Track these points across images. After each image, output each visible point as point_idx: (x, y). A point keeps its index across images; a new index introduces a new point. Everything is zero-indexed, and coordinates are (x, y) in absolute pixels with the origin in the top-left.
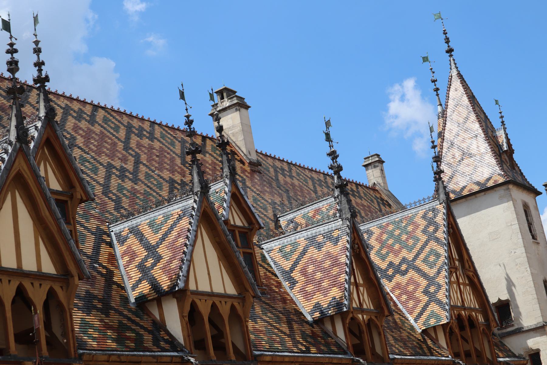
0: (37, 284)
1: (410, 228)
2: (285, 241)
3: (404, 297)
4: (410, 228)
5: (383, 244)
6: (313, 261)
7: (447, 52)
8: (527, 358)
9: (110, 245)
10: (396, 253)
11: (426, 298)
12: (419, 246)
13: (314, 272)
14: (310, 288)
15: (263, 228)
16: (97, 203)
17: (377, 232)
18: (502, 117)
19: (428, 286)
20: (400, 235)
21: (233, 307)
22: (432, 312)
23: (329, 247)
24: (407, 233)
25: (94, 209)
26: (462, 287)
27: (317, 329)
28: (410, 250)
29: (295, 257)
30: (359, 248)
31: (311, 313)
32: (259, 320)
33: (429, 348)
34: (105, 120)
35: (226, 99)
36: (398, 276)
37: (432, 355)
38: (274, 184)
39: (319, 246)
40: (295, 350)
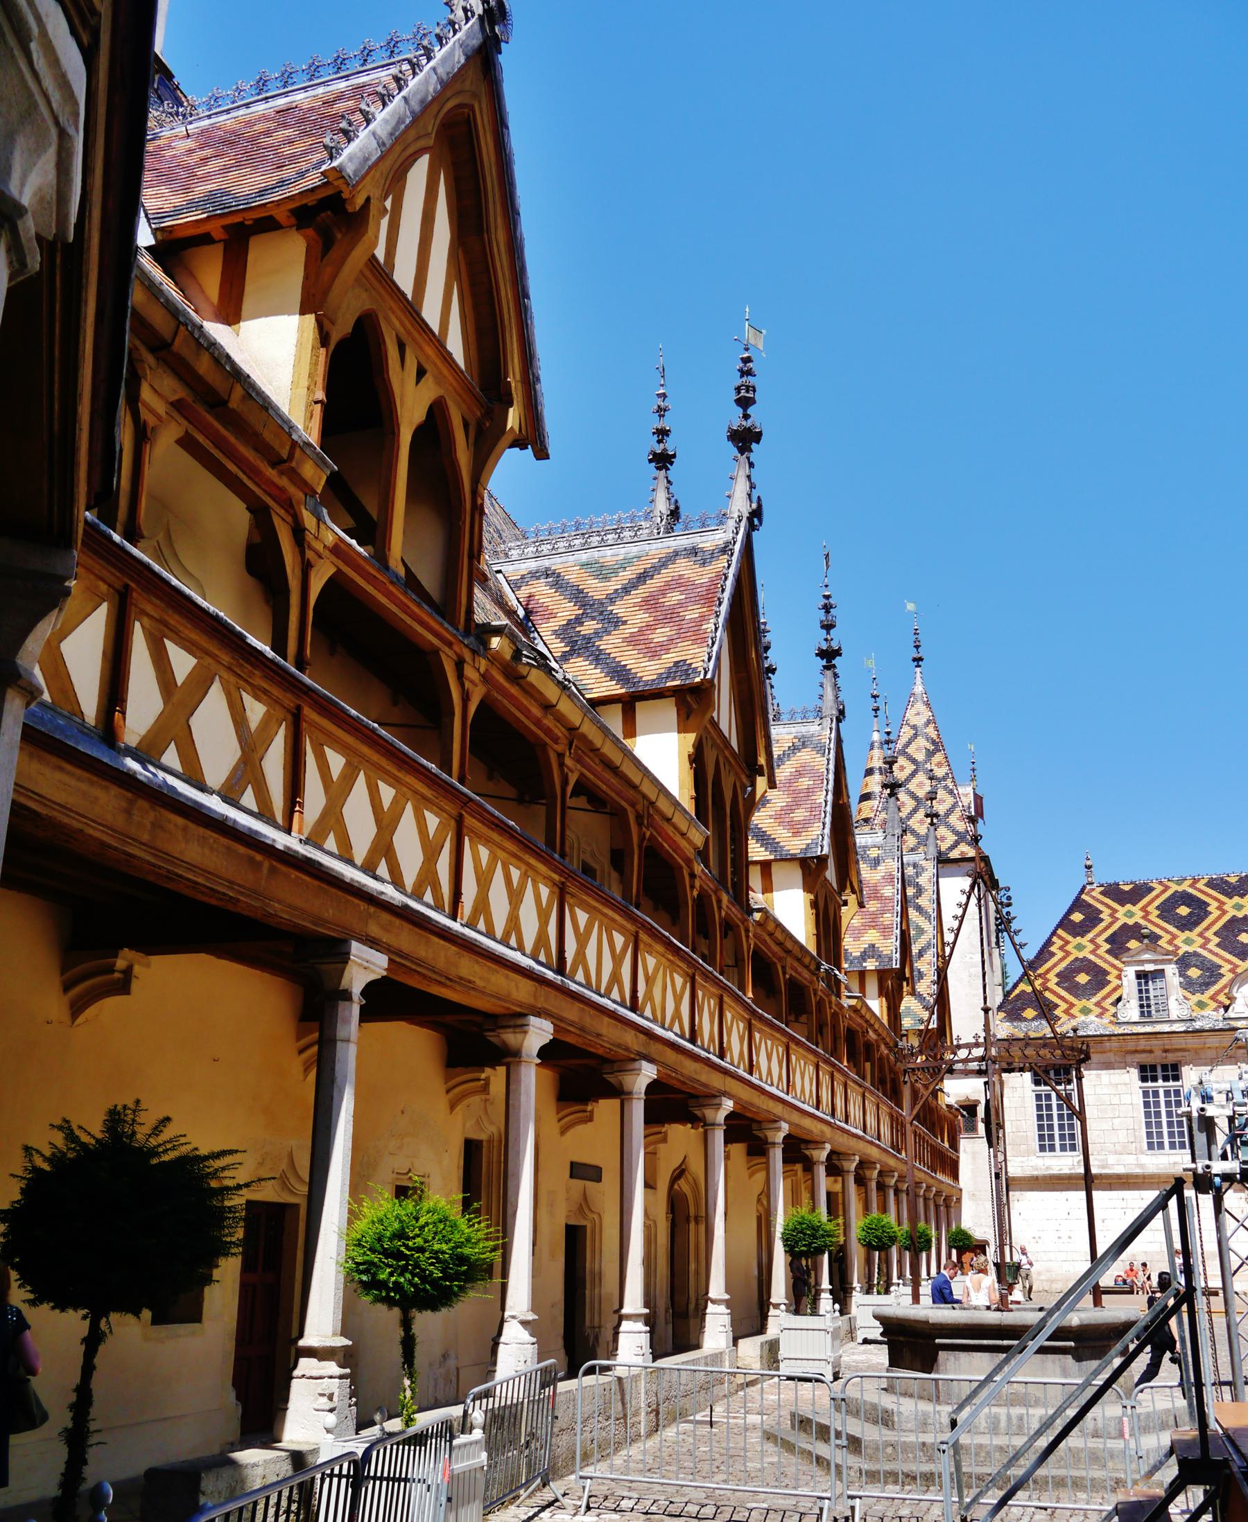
7: (914, 660)
18: (974, 770)
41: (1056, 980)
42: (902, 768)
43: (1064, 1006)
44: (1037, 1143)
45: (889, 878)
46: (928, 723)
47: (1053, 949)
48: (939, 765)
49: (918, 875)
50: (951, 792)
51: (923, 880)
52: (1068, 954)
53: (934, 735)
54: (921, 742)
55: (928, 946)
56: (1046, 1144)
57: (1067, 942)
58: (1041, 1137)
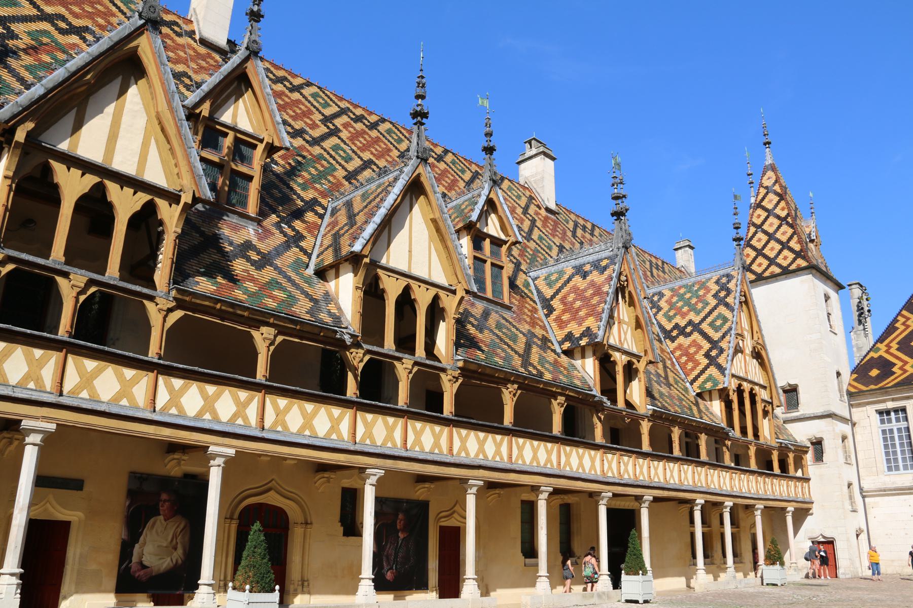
0: (129, 191)
1: (701, 293)
2: (553, 269)
3: (684, 359)
4: (701, 293)
5: (672, 305)
6: (575, 289)
7: (765, 144)
8: (809, 445)
9: (322, 217)
10: (684, 315)
11: (706, 361)
12: (707, 310)
13: (575, 300)
14: (565, 317)
15: (520, 243)
16: (329, 181)
17: (668, 293)
19: (710, 350)
20: (690, 298)
21: (436, 298)
23: (595, 277)
24: (697, 297)
26: (747, 358)
27: (564, 359)
28: (698, 313)
29: (559, 285)
30: (627, 280)
31: (561, 343)
32: (486, 331)
33: (700, 411)
34: (389, 131)
35: (533, 149)
38: (569, 234)
39: (585, 275)
40: (522, 370)
41: (897, 346)
42: (759, 216)
43: (900, 364)
46: (776, 182)
47: (897, 325)
48: (783, 209)
49: (728, 282)
50: (791, 226)
51: (731, 286)
52: (908, 327)
53: (779, 191)
54: (771, 196)
55: (730, 329)
57: (908, 319)
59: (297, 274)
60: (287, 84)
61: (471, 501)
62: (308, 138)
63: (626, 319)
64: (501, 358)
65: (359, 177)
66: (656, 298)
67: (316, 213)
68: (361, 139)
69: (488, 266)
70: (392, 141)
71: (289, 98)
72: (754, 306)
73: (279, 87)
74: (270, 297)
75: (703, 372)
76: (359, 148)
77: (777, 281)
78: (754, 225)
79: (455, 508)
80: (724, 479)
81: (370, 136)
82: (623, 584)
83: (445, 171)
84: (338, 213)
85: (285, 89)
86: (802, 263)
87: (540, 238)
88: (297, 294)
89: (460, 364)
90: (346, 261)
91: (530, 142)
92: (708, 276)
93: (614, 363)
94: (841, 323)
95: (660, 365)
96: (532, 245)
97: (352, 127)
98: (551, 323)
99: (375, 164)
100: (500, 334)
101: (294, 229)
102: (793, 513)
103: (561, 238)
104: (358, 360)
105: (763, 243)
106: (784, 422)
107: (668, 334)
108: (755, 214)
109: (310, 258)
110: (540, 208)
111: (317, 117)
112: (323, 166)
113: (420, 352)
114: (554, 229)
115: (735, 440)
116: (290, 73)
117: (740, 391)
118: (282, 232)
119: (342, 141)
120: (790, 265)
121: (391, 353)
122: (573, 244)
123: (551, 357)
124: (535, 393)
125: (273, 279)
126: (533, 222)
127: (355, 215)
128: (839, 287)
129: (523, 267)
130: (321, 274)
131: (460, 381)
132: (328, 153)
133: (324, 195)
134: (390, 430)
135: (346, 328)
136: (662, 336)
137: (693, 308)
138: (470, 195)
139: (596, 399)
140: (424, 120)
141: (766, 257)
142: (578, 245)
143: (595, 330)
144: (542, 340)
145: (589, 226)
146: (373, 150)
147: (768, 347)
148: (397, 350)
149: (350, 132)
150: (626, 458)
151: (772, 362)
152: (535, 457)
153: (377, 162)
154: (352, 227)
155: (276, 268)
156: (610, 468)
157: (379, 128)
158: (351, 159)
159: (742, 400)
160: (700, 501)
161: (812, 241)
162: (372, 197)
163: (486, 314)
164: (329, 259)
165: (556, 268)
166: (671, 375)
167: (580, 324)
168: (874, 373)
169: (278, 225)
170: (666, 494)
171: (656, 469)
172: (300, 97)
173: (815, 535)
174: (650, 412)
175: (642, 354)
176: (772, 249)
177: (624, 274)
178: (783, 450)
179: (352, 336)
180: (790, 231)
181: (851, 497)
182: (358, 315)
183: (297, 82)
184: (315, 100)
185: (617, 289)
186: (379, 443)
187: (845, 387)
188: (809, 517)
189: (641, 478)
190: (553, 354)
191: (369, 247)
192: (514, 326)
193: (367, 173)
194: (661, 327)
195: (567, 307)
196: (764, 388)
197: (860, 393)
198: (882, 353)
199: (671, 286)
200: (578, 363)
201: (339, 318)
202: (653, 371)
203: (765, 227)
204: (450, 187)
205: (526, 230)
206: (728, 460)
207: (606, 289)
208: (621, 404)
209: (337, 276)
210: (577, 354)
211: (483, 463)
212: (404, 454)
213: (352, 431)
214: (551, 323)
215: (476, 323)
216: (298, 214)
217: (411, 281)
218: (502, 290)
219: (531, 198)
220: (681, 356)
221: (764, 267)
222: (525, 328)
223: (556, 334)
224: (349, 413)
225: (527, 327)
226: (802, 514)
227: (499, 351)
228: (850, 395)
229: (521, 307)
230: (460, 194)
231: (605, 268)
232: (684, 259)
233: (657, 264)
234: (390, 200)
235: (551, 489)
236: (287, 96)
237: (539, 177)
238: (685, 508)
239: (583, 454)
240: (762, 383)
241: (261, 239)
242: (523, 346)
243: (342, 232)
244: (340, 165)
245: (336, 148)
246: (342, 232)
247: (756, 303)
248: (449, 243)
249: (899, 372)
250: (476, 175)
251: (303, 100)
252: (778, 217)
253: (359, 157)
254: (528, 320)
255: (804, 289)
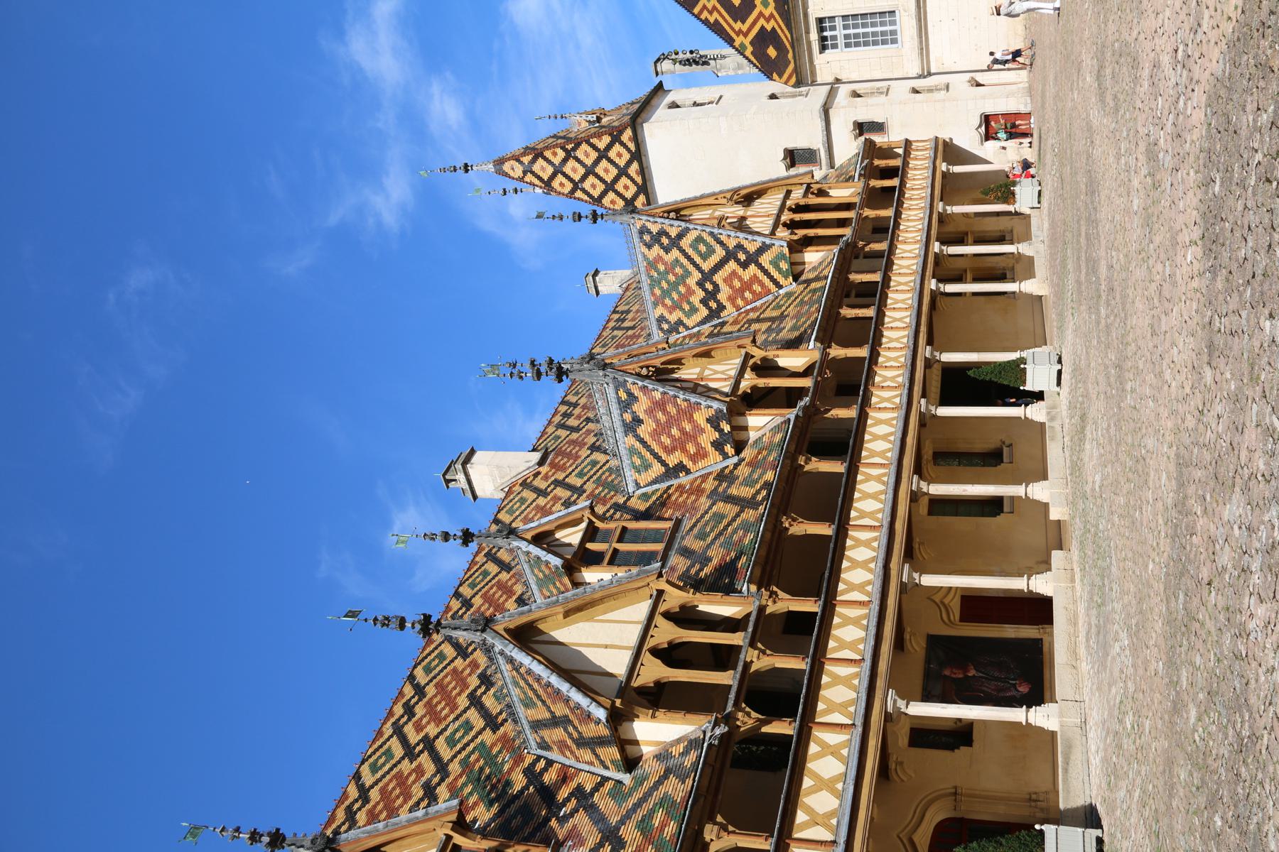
1: (662, 268)
2: (626, 462)
3: (748, 295)
4: (662, 268)
5: (676, 306)
6: (656, 434)
7: (467, 171)
8: (862, 139)
9: (550, 763)
10: (690, 292)
11: (753, 268)
13: (670, 435)
14: (691, 449)
16: (500, 752)
17: (660, 311)
19: (737, 261)
20: (668, 282)
21: (668, 615)
22: (771, 262)
23: (640, 408)
25: (503, 763)
26: (749, 213)
27: (747, 453)
29: (648, 455)
30: (647, 367)
31: (726, 456)
32: (709, 553)
33: (817, 279)
34: (428, 670)
36: (719, 296)
37: (826, 278)
38: (575, 436)
39: (638, 421)
40: (761, 508)
42: (562, 185)
43: (762, 22)
44: (890, 46)
45: (644, 388)
46: (518, 160)
47: (712, 20)
48: (555, 154)
49: (649, 232)
50: (578, 145)
51: (654, 229)
53: (530, 157)
55: (711, 234)
56: (890, 39)
57: (705, 7)
58: (884, 42)
59: (630, 795)
60: (356, 806)
61: (929, 580)
62: (436, 779)
63: (697, 370)
64: (745, 536)
65: (494, 713)
66: (665, 326)
67: (545, 770)
68: (439, 708)
69: (622, 547)
70: (441, 666)
71: (378, 803)
72: (682, 201)
73: (361, 817)
74: (662, 830)
75: (766, 272)
76: (452, 712)
77: (649, 167)
78: (573, 191)
79: (937, 600)
80: (906, 251)
81: (435, 696)
82: (1037, 389)
83: (485, 597)
84: (547, 739)
85: (364, 810)
86: (627, 135)
87: (581, 475)
88: (657, 795)
89: (753, 588)
90: (616, 730)
91: (448, 482)
92: (640, 257)
93: (754, 388)
94: (706, 88)
95: (755, 326)
96: (589, 487)
97: (421, 719)
98: (699, 468)
99: (475, 690)
100: (712, 535)
101: (568, 799)
102: (949, 164)
103: (581, 448)
104: (746, 719)
105: (597, 182)
106: (832, 167)
107: (714, 314)
108: (559, 189)
109: (608, 779)
110: (537, 475)
111: (406, 766)
112: (478, 760)
113: (737, 639)
114: (569, 455)
115: (856, 233)
116: (341, 802)
117: (792, 225)
118: (572, 815)
119: (441, 733)
120: (628, 150)
121: (738, 676)
122: (589, 432)
123: (743, 471)
124: (793, 492)
125: (638, 826)
126: (557, 483)
127: (554, 717)
128: (659, 89)
129: (621, 501)
130: (630, 763)
131: (775, 589)
132: (459, 752)
133: (519, 759)
134: (837, 680)
135: (704, 732)
136: (716, 321)
137: (682, 279)
138: (526, 566)
139: (800, 414)
140: (434, 620)
141: (616, 179)
142: (591, 426)
143: (711, 412)
144: (721, 482)
145: (563, 409)
146: (454, 693)
147: (736, 185)
148: (734, 668)
149: (428, 723)
150: (877, 379)
151: (755, 181)
152: (874, 496)
153: (471, 688)
154: (570, 722)
155: (622, 822)
156: (888, 400)
157: (423, 684)
158: (467, 722)
159: (804, 223)
160: (933, 284)
161: (599, 119)
162: (531, 694)
163: (686, 552)
164: (612, 753)
165: (624, 458)
166: (768, 314)
167: (703, 431)
168: (772, 52)
169: (563, 820)
170: (923, 329)
171: (891, 340)
172: (377, 788)
173: (977, 137)
174: (819, 345)
175: (743, 351)
176: (606, 171)
177: (638, 370)
178: (871, 172)
179: (716, 724)
180: (584, 147)
181: (930, 91)
182: (689, 716)
183: (353, 792)
184: (381, 768)
185: (659, 381)
186: (854, 695)
187: (790, 89)
188: (955, 142)
189: (903, 360)
190: (740, 468)
191: (601, 699)
192: (702, 516)
193: (489, 701)
194: (703, 322)
195: (679, 445)
196: (788, 193)
197: (797, 71)
198: (747, 41)
199: (650, 305)
200: (753, 436)
201: (691, 742)
202: (764, 337)
203: (577, 178)
204: (510, 592)
205: (569, 493)
206: (883, 246)
207: (657, 395)
208: (807, 382)
209: (636, 743)
210: (742, 436)
211: (880, 564)
212: (867, 664)
213: (838, 729)
214: (699, 468)
215: (697, 566)
216: (548, 794)
217: (646, 648)
218: (653, 529)
219: (525, 484)
220: (743, 298)
221: (629, 182)
222: (704, 502)
223: (714, 462)
224: (817, 733)
225: (703, 499)
226: (950, 152)
227: (735, 538)
228: (799, 84)
229: (678, 506)
230: (519, 577)
231: (630, 394)
232: (610, 284)
233: (617, 320)
234: (539, 669)
235: (916, 477)
236: (375, 807)
237: (496, 472)
238: (941, 302)
239: (871, 434)
240: (781, 196)
241: (581, 843)
242: (729, 506)
243: (575, 735)
244: (476, 737)
245: (451, 742)
246: (575, 735)
247: (679, 198)
248: (597, 596)
249: (772, 23)
250: (491, 557)
251: (381, 784)
252: (565, 161)
253: (465, 711)
254: (693, 497)
255: (660, 134)
